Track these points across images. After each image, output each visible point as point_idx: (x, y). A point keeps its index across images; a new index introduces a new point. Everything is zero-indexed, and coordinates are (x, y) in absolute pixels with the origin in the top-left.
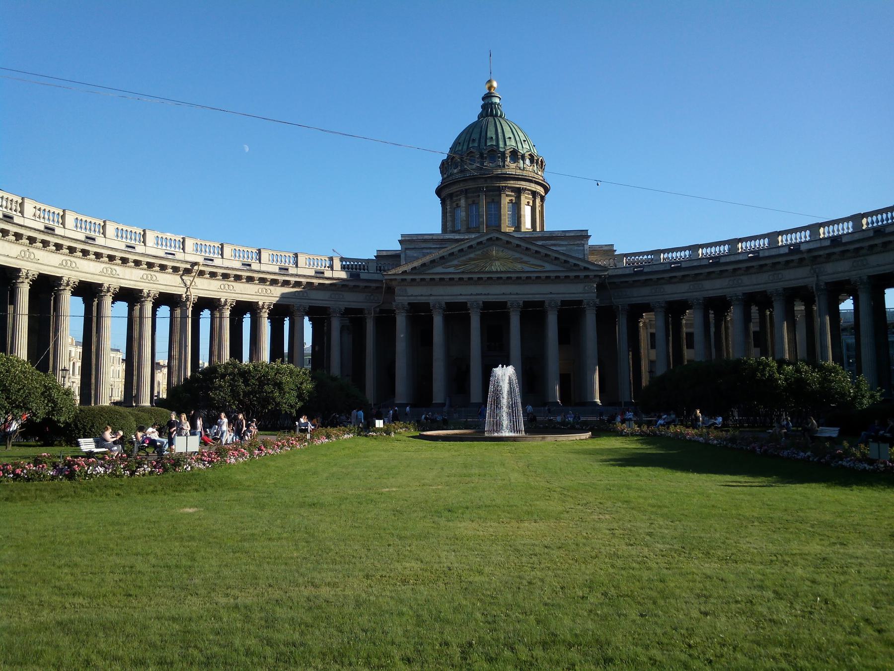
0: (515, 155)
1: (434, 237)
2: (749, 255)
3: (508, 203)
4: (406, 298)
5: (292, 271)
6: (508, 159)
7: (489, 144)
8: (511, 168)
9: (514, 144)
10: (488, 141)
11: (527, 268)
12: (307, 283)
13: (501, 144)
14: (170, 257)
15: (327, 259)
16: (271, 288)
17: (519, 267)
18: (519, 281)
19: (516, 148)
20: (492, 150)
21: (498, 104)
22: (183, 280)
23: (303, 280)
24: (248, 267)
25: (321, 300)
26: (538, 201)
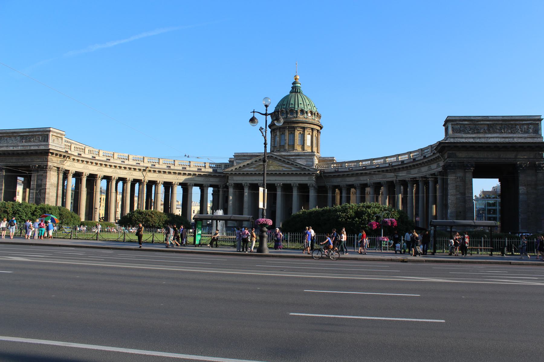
0: (302, 111)
1: (248, 154)
2: (377, 166)
3: (299, 134)
4: (233, 181)
5: (188, 168)
6: (299, 114)
7: (290, 106)
8: (301, 117)
9: (302, 106)
10: (290, 105)
11: (284, 169)
12: (193, 174)
13: (296, 107)
14: (138, 165)
15: (203, 163)
16: (179, 176)
17: (281, 168)
18: (280, 175)
19: (303, 109)
20: (292, 110)
21: (299, 87)
22: (143, 174)
23: (192, 173)
24: (169, 168)
25: (200, 180)
26: (315, 132)
